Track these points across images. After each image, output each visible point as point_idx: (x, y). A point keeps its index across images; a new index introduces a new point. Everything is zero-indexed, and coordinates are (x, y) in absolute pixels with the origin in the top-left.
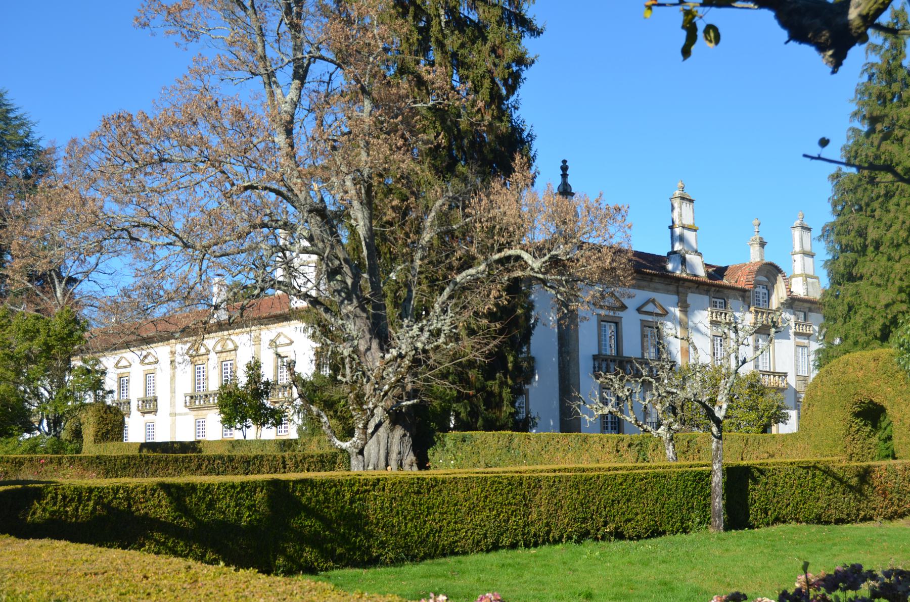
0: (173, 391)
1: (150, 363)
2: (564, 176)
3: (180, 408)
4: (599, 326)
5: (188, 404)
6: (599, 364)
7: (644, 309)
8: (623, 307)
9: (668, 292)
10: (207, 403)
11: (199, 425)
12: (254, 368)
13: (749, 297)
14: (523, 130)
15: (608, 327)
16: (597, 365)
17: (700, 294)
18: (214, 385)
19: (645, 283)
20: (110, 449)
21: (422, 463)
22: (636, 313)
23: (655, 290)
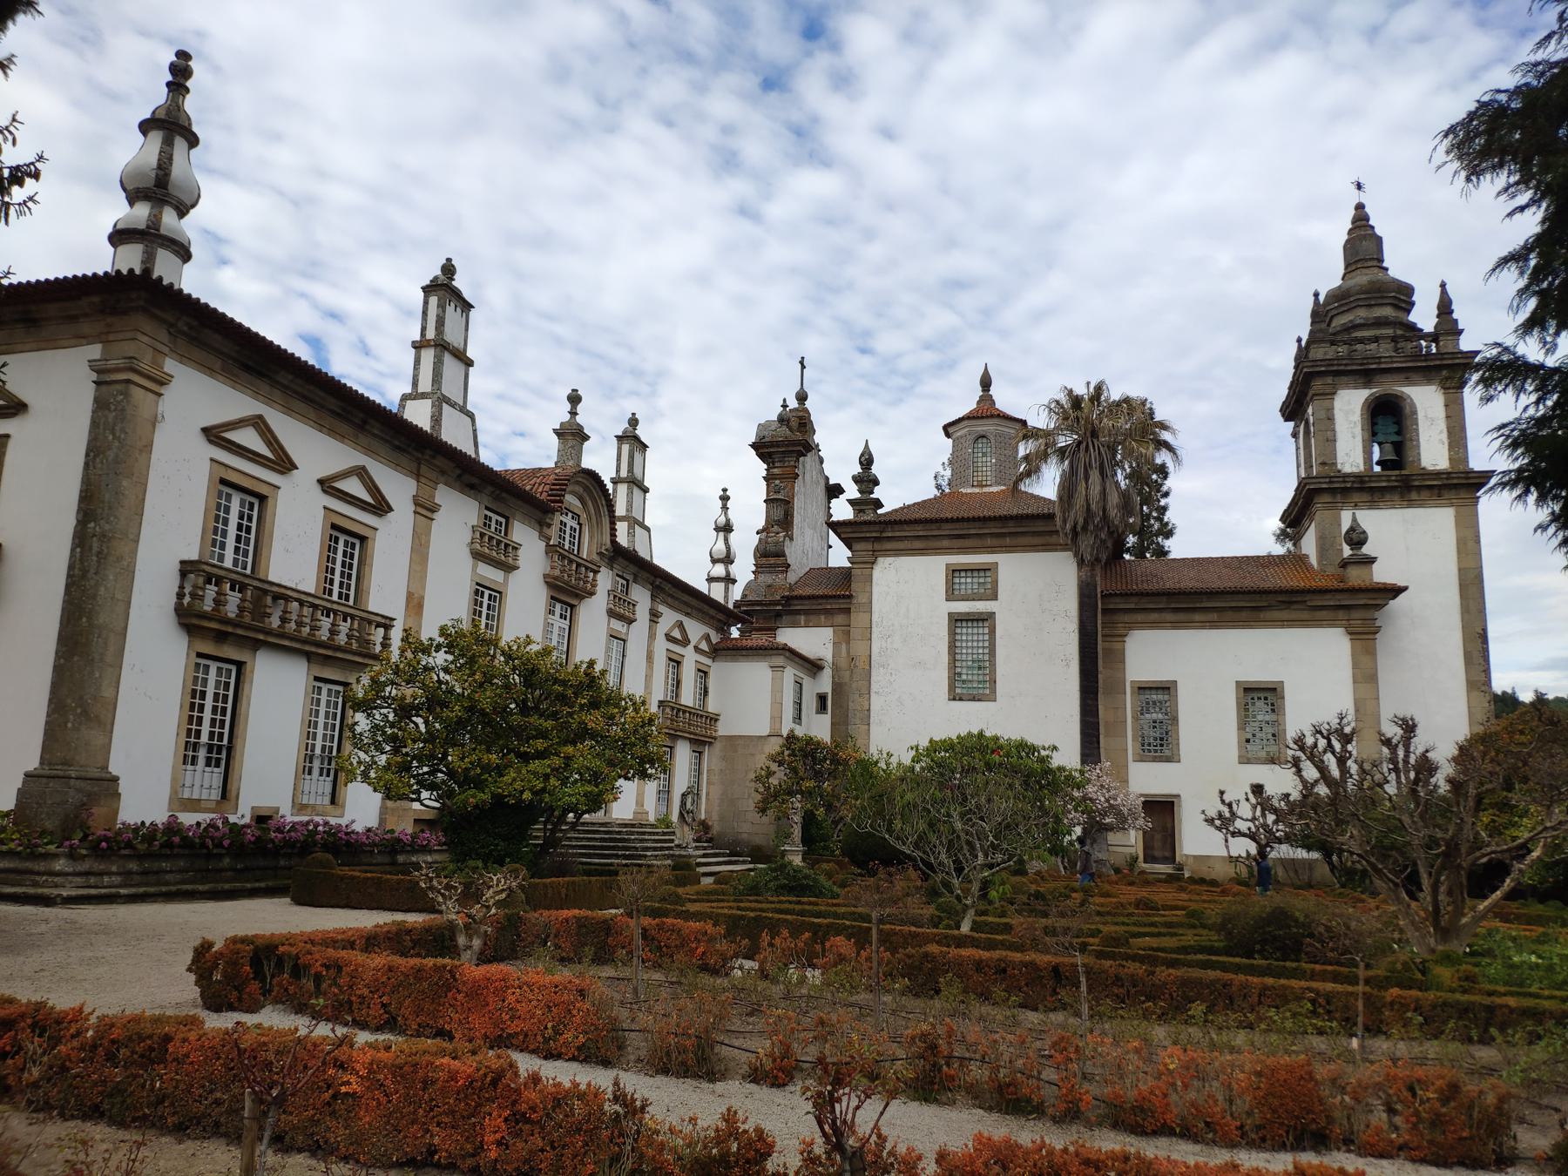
6: (195, 587)
8: (283, 463)
9: (397, 466)
22: (318, 489)
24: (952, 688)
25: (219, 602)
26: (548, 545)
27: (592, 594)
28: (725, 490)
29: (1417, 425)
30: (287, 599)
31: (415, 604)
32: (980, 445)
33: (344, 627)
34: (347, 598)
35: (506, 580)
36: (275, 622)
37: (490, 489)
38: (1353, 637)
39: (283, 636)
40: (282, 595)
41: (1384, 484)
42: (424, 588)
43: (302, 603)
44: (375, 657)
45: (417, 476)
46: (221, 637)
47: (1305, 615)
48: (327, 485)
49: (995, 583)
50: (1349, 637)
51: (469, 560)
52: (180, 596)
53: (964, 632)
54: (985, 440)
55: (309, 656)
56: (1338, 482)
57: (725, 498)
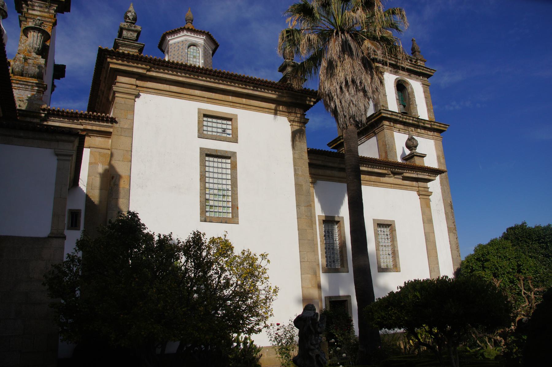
24: (203, 211)
29: (415, 98)
32: (192, 50)
38: (421, 196)
41: (411, 122)
47: (400, 181)
49: (235, 131)
50: (419, 197)
53: (211, 162)
54: (195, 48)
56: (395, 115)
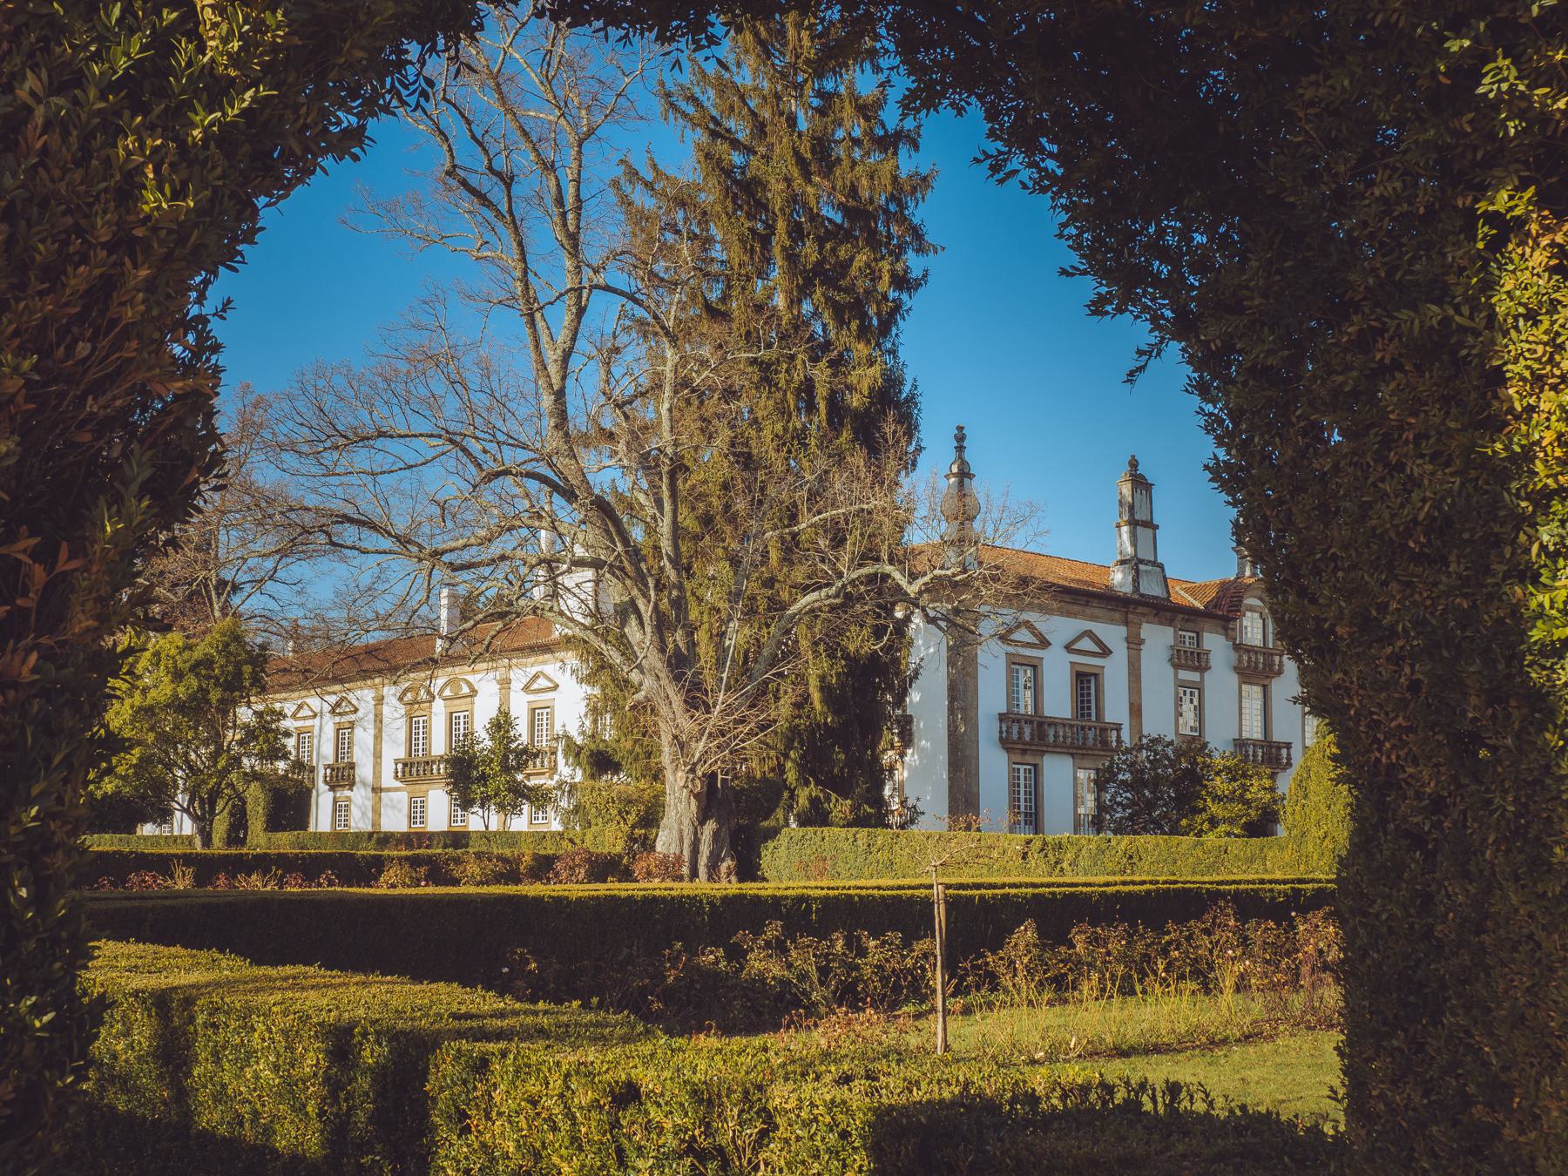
0: (378, 755)
1: (305, 718)
2: (960, 449)
3: (388, 780)
4: (1009, 671)
5: (400, 774)
7: (1075, 646)
8: (1044, 643)
9: (1112, 621)
10: (428, 774)
11: (417, 810)
12: (501, 725)
13: (1233, 630)
14: (901, 383)
15: (1021, 673)
16: (1004, 729)
17: (1161, 623)
18: (439, 746)
19: (1076, 608)
20: (284, 842)
21: (748, 870)
23: (1093, 618)
25: (1021, 733)
26: (1234, 644)
27: (1280, 673)
28: (960, 429)
30: (1055, 724)
31: (1136, 711)
33: (1091, 734)
34: (1089, 715)
35: (1202, 678)
36: (1051, 739)
37: (1180, 616)
39: (1056, 746)
40: (1053, 723)
42: (1140, 698)
43: (1064, 725)
44: (1113, 750)
45: (1126, 623)
46: (1024, 752)
48: (1068, 648)
51: (1171, 670)
52: (1001, 732)
55: (1072, 755)
57: (960, 438)
